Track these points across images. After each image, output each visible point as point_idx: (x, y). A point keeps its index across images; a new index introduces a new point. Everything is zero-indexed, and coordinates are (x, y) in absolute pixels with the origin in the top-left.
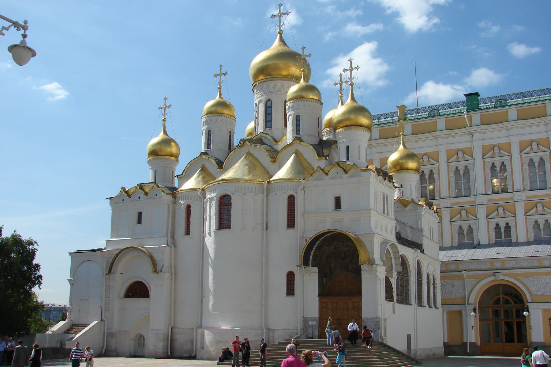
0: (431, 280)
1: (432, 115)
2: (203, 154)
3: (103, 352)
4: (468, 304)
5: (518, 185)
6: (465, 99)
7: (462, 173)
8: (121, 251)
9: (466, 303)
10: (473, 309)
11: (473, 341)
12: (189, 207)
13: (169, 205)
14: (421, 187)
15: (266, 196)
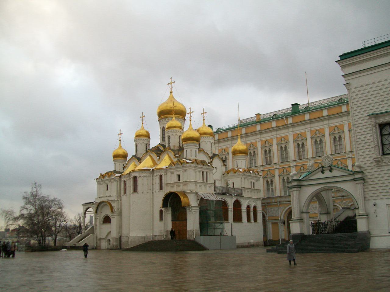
0: (252, 209)
1: (274, 117)
2: (133, 156)
3: (95, 247)
4: (280, 219)
5: (310, 155)
6: (291, 106)
7: (284, 149)
8: (100, 203)
9: (280, 218)
10: (282, 222)
11: (283, 238)
12: (125, 181)
13: (117, 181)
14: (266, 158)
15: (153, 176)
